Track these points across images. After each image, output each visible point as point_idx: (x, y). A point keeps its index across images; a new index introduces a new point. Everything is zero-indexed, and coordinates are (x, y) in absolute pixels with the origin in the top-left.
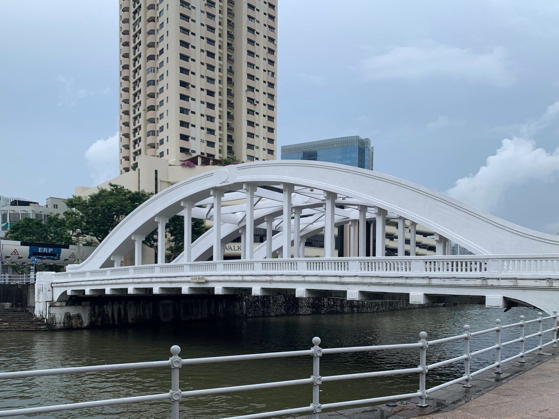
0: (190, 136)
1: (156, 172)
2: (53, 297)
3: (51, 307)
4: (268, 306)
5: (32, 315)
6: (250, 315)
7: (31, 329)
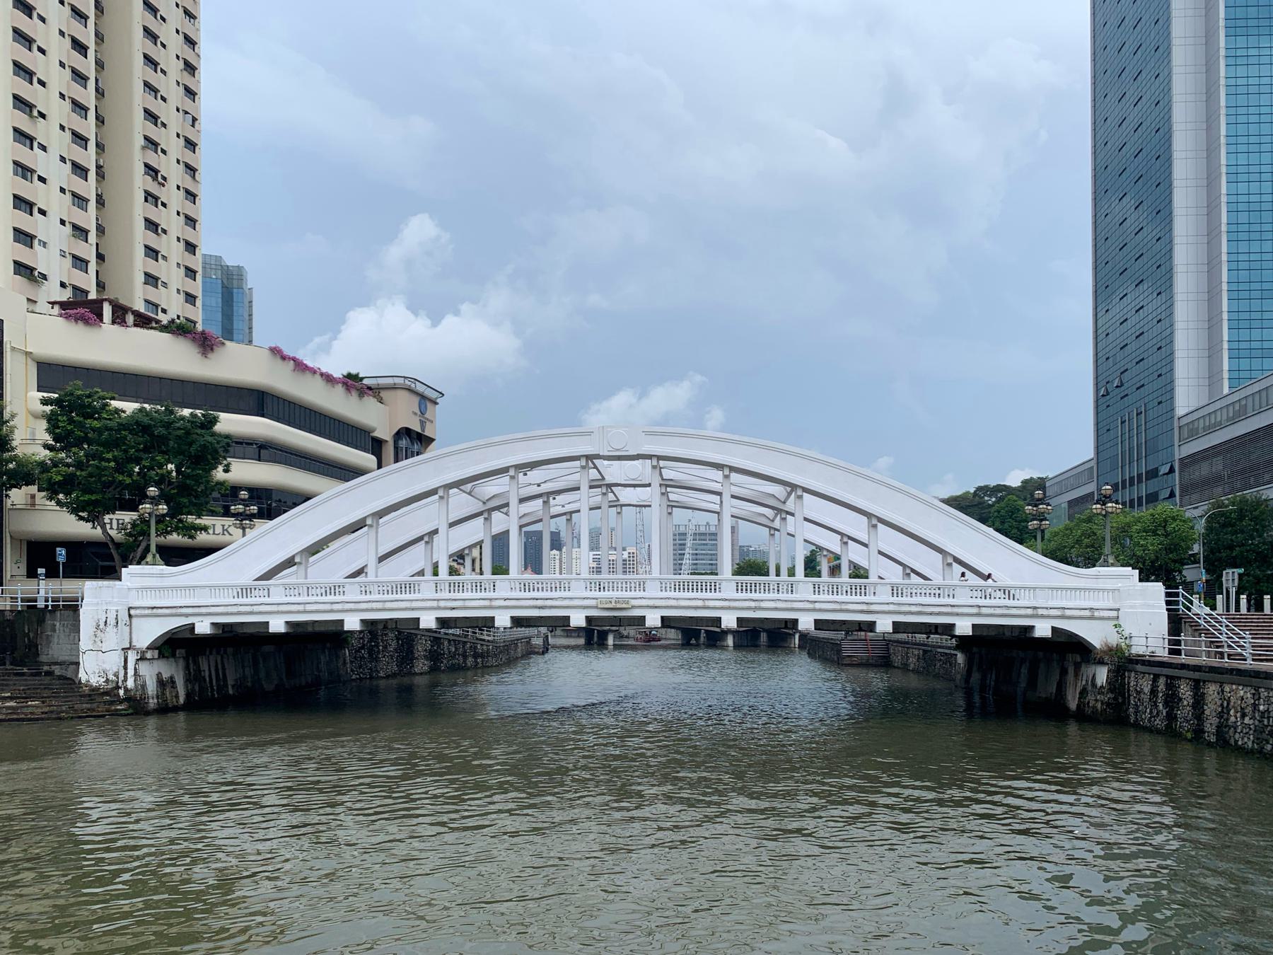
2: (131, 639)
3: (140, 662)
5: (71, 683)
7: (99, 711)
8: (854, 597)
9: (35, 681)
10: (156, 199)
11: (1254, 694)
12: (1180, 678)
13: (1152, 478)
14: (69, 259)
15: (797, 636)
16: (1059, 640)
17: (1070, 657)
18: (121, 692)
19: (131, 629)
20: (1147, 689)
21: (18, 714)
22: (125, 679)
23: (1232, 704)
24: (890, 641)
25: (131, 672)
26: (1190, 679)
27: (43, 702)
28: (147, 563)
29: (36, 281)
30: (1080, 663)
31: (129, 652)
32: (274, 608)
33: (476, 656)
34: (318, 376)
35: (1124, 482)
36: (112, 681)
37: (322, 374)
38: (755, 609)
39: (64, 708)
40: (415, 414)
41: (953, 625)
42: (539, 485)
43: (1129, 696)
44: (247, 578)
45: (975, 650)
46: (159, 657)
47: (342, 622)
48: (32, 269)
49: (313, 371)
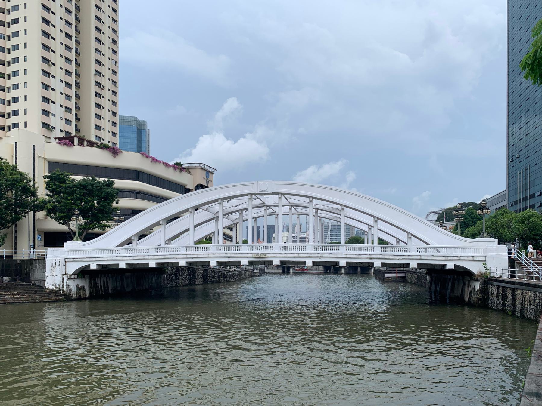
0: (50, 112)
1: (34, 146)
3: (69, 280)
4: (179, 278)
5: (42, 288)
6: (168, 286)
7: (51, 299)
8: (383, 252)
9: (28, 287)
10: (100, 95)
11: (534, 295)
12: (507, 287)
13: (532, 198)
14: (64, 121)
15: (373, 269)
16: (460, 270)
17: (466, 278)
18: (61, 292)
19: (66, 267)
20: (495, 292)
21: (19, 300)
22: (63, 287)
23: (526, 299)
24: (406, 271)
25: (65, 284)
26: (511, 288)
27: (30, 296)
28: (74, 241)
29: (50, 130)
30: (470, 280)
31: (65, 276)
32: (121, 258)
33: (224, 277)
34: (162, 164)
35: (520, 200)
36: (58, 287)
37: (164, 163)
38: (320, 257)
39: (38, 298)
40: (204, 178)
41: (409, 264)
42: (236, 206)
43: (489, 295)
44: (113, 246)
45: (433, 275)
46: (77, 278)
47: (148, 264)
48: (49, 125)
49: (160, 162)
